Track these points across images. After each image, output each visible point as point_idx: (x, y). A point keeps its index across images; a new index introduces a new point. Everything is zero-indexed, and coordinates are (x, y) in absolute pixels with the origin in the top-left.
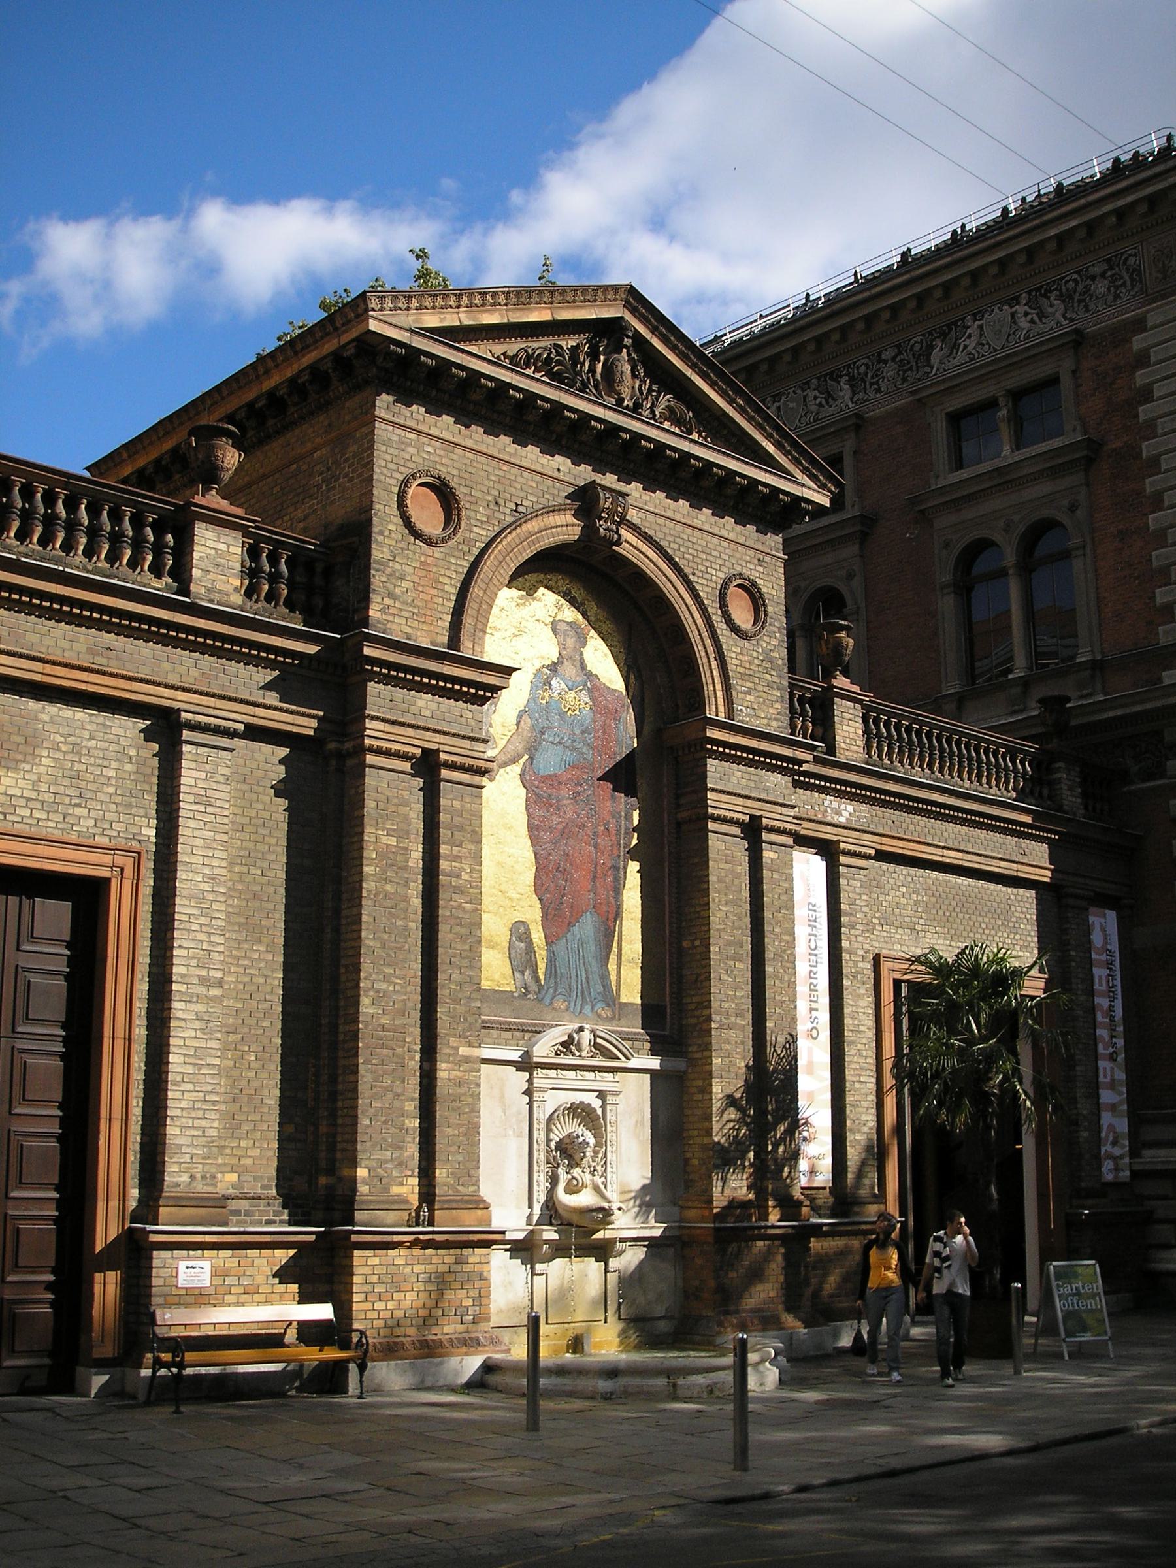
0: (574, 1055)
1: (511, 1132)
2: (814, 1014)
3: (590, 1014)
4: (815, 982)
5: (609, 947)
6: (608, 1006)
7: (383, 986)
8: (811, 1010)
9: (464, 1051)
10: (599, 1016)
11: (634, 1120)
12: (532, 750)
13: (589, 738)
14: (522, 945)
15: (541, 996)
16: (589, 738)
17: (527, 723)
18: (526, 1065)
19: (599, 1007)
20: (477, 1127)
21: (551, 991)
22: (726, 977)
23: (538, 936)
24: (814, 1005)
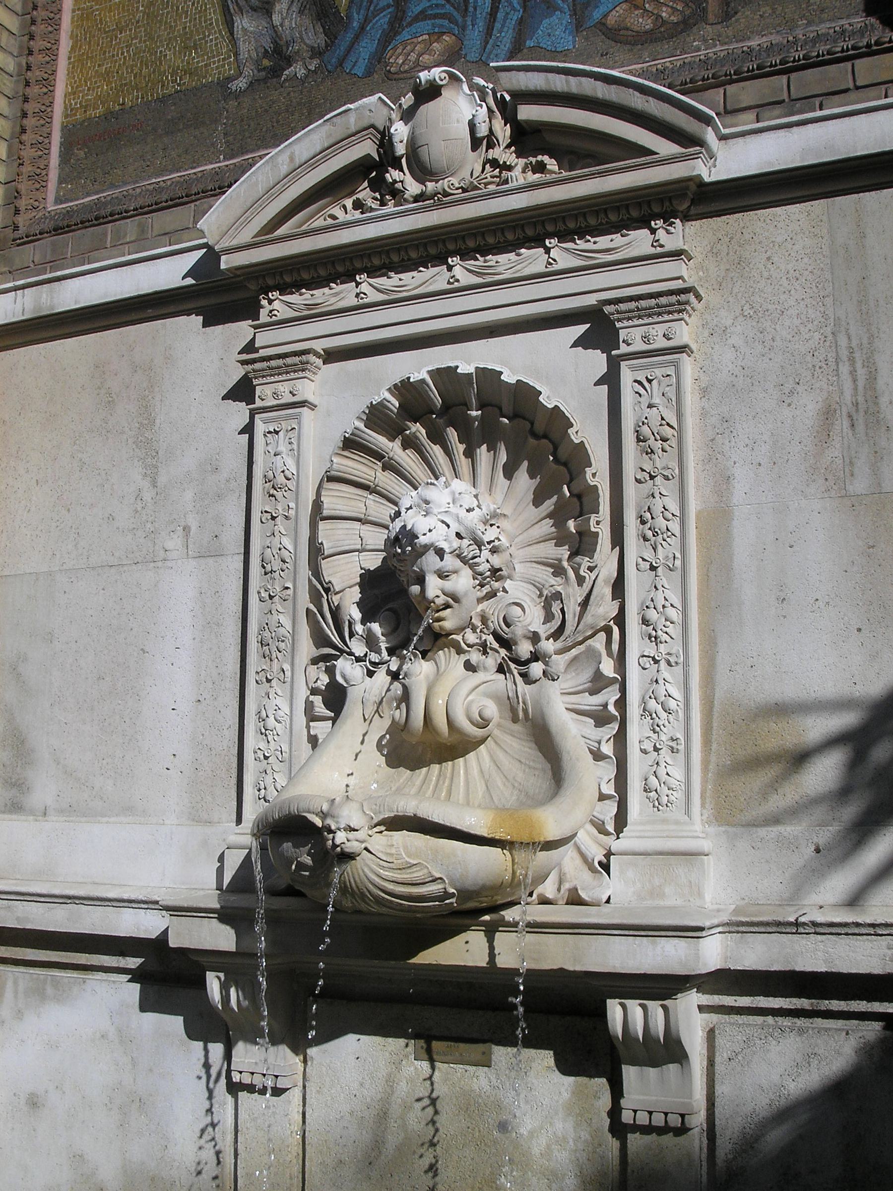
0: (395, 193)
1: (174, 543)
3: (567, 42)
11: (809, 405)
18: (221, 295)
21: (383, 20)
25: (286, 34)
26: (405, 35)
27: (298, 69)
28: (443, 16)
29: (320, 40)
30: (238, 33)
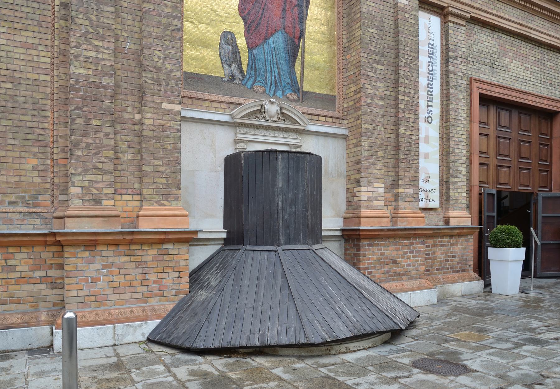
2: (430, 108)
3: (281, 96)
4: (431, 90)
5: (295, 56)
6: (295, 92)
7: (93, 54)
8: (428, 106)
9: (166, 106)
10: (288, 98)
14: (230, 48)
15: (244, 82)
19: (288, 93)
20: (178, 162)
21: (252, 79)
23: (241, 42)
24: (430, 104)
26: (256, 84)
27: (236, 81)
29: (241, 78)
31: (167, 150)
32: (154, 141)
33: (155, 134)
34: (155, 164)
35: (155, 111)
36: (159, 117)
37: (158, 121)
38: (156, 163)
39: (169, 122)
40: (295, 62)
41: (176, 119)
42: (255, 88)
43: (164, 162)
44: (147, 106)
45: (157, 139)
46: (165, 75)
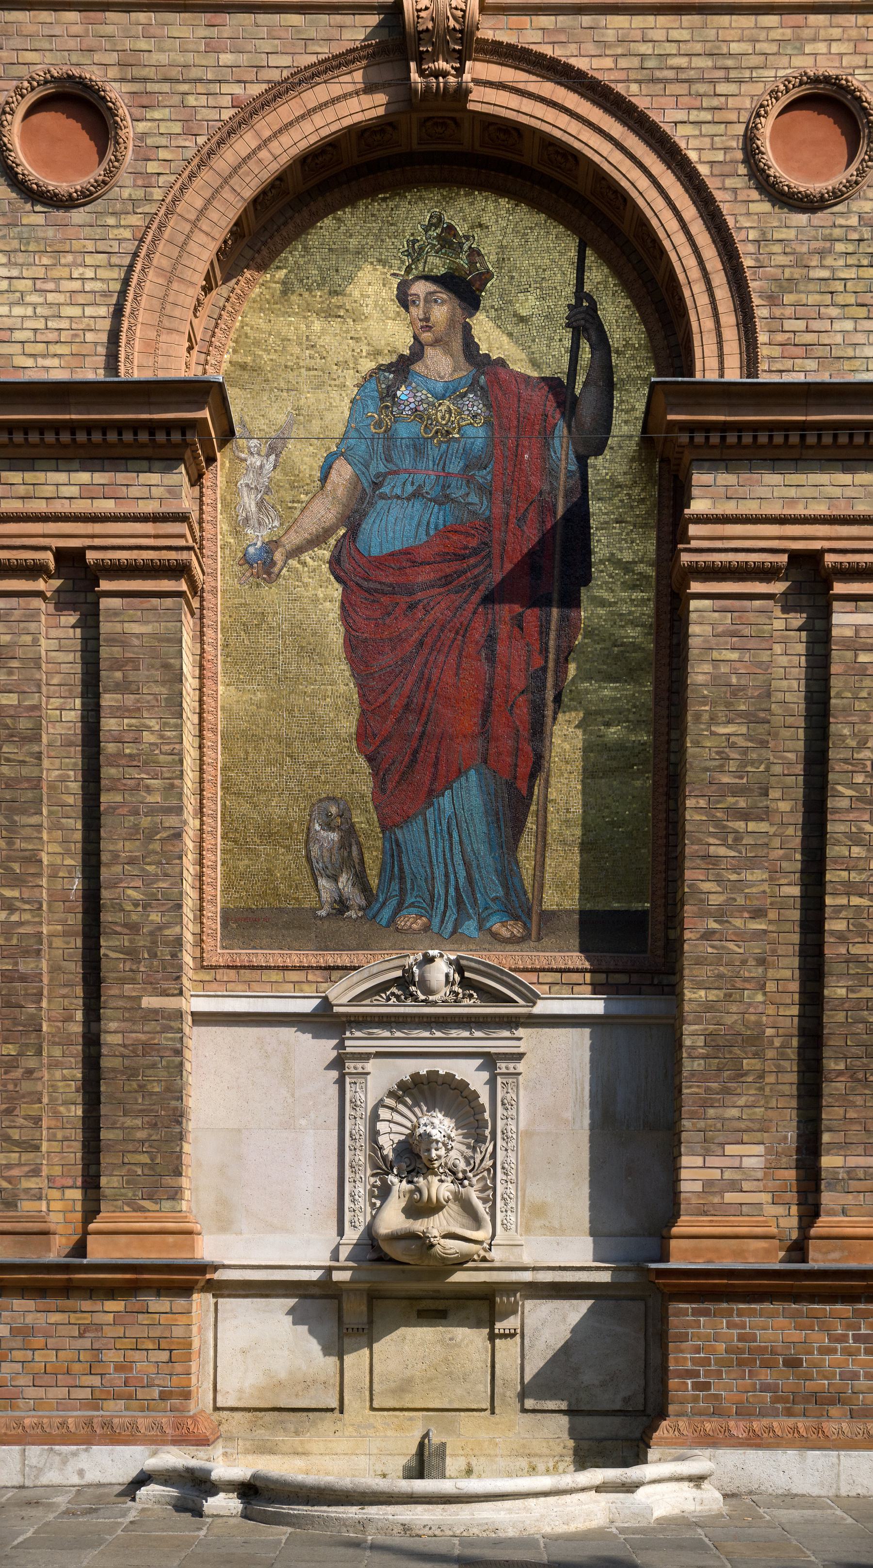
12: (353, 520)
13: (482, 476)
14: (334, 836)
16: (482, 476)
17: (343, 472)
20: (178, 1117)
21: (394, 902)
22: (722, 851)
25: (346, 895)
26: (405, 912)
27: (352, 914)
28: (422, 908)
29: (363, 903)
30: (320, 887)
31: (152, 1094)
32: (124, 1077)
33: (127, 1062)
34: (126, 1125)
35: (127, 1015)
36: (135, 1028)
37: (134, 1035)
38: (129, 1122)
39: (157, 1036)
40: (517, 841)
41: (172, 1028)
42: (401, 923)
43: (146, 1119)
44: (111, 1006)
45: (131, 1073)
46: (148, 938)
